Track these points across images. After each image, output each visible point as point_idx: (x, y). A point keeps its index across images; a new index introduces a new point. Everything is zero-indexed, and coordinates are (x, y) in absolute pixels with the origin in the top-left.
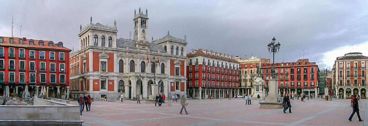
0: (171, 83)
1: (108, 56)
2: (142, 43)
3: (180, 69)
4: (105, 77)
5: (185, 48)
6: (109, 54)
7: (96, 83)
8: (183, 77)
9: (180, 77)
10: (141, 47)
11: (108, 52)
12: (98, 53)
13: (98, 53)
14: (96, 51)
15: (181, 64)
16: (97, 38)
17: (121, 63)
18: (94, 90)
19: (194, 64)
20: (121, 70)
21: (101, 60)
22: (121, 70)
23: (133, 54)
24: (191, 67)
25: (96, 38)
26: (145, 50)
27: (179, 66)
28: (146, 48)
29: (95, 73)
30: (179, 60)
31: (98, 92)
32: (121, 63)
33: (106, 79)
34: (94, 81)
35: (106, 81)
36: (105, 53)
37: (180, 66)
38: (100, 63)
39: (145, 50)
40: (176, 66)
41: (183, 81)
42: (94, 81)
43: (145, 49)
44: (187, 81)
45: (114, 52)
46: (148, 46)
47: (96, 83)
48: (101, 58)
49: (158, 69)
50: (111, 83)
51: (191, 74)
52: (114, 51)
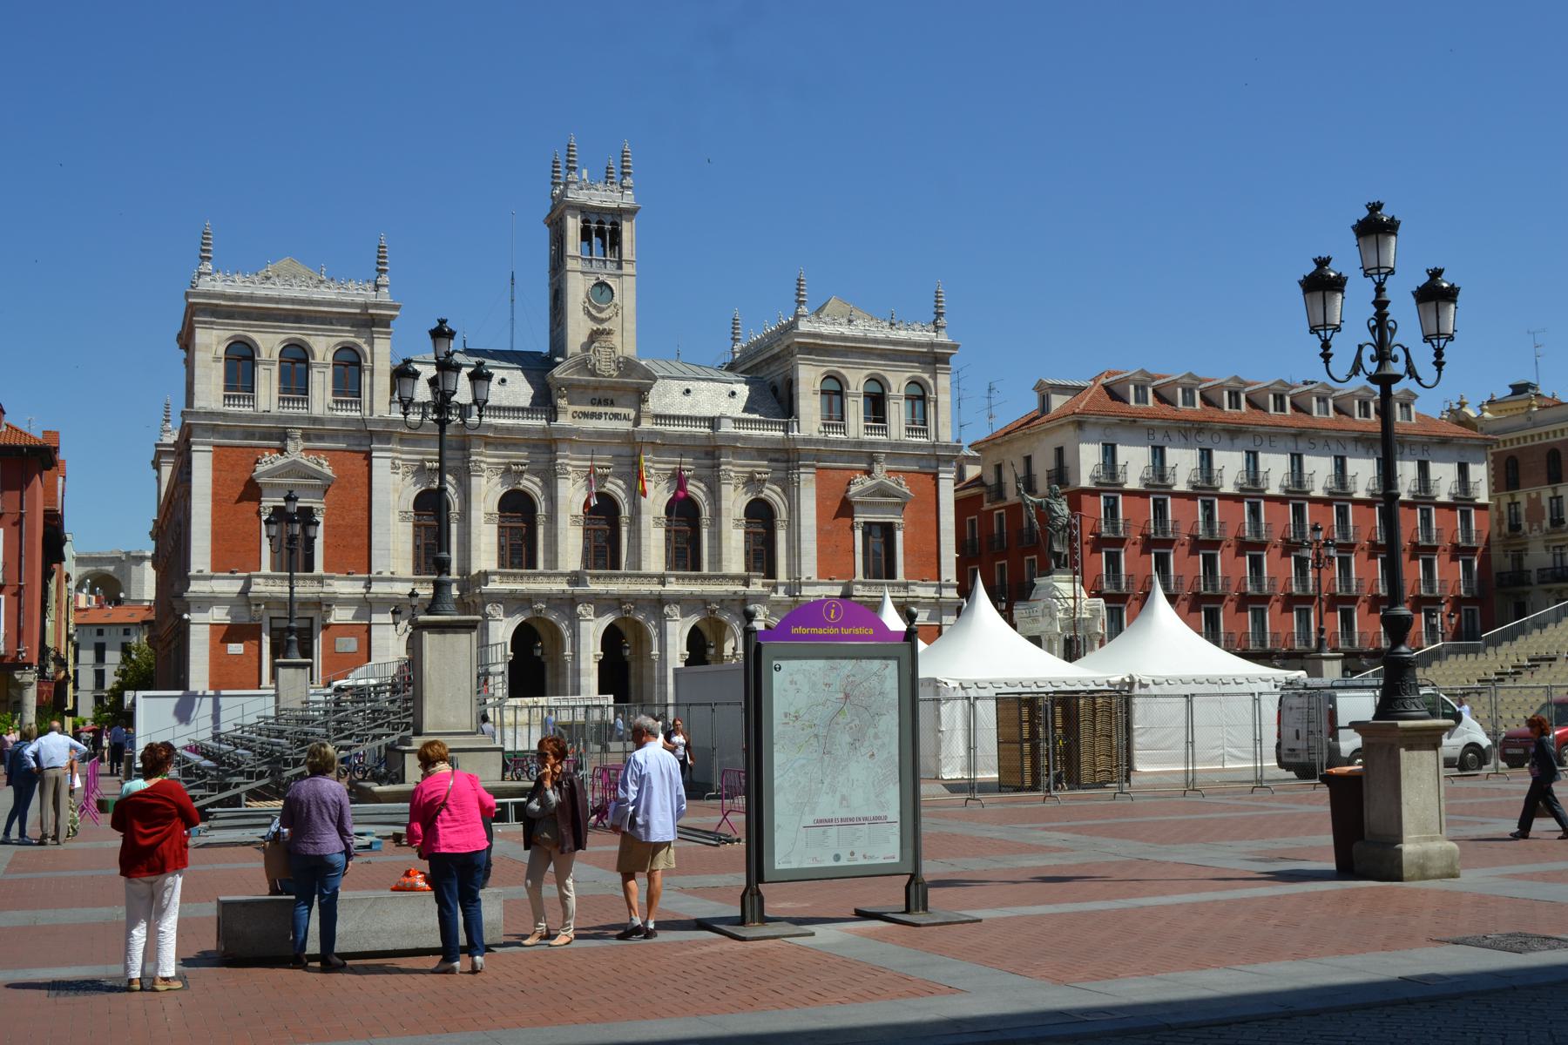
3: (899, 535)
47: (236, 648)
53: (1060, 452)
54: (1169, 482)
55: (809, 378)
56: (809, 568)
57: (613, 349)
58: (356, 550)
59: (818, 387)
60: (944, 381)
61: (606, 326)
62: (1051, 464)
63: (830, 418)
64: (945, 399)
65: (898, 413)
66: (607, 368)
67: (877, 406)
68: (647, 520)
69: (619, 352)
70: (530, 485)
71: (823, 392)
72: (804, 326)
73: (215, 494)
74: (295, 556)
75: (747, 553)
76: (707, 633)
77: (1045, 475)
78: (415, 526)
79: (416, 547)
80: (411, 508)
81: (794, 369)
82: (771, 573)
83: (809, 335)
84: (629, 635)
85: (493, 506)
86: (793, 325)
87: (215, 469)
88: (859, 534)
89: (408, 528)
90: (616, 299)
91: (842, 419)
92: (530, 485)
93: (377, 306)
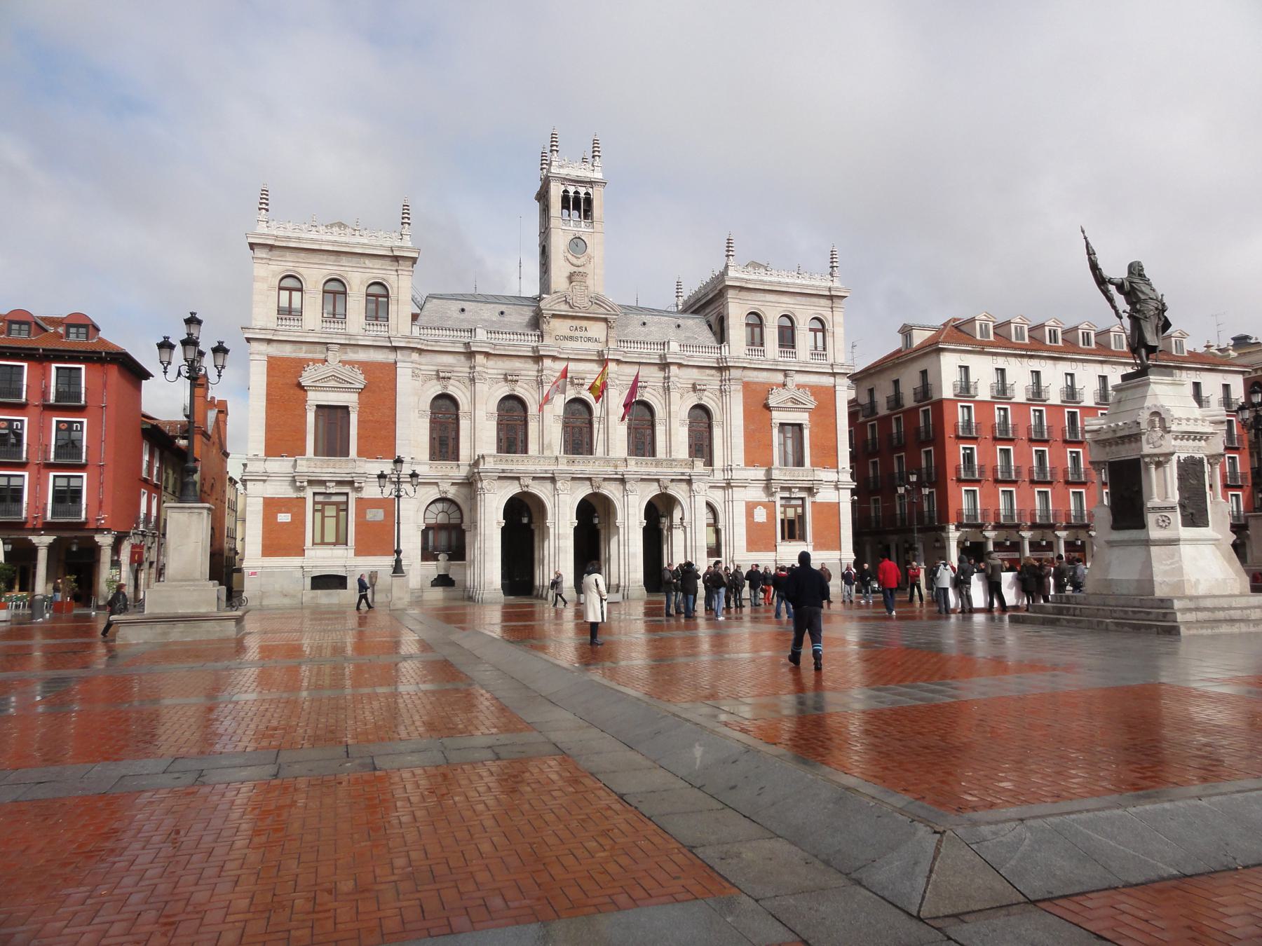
0: (750, 508)
1: (362, 377)
2: (566, 307)
3: (806, 433)
4: (339, 483)
5: (838, 321)
6: (365, 367)
7: (284, 518)
8: (828, 475)
9: (805, 474)
10: (561, 327)
11: (362, 356)
12: (300, 365)
13: (300, 365)
14: (287, 351)
15: (809, 406)
16: (301, 290)
17: (445, 413)
18: (270, 549)
19: (909, 401)
20: (444, 443)
21: (315, 398)
22: (444, 443)
23: (517, 364)
24: (898, 419)
25: (290, 290)
26: (589, 339)
27: (802, 418)
28: (597, 330)
29: (280, 465)
30: (799, 387)
31: (296, 561)
32: (445, 413)
33: (347, 494)
34: (272, 506)
35: (347, 503)
36: (344, 363)
37: (806, 415)
38: (311, 417)
39: (589, 339)
40: (778, 417)
41: (826, 495)
42: (272, 506)
43: (589, 334)
44: (854, 492)
45: (400, 355)
46: (605, 320)
47: (284, 518)
48: (316, 389)
49: (674, 436)
50: (376, 515)
51: (900, 458)
52: (395, 349)
53: (924, 373)
54: (1009, 395)
55: (737, 312)
56: (739, 456)
57: (587, 287)
58: (381, 439)
59: (744, 321)
60: (839, 317)
61: (581, 269)
62: (917, 383)
63: (753, 344)
64: (840, 331)
65: (804, 339)
66: (582, 302)
67: (787, 338)
68: (675, 424)
69: (591, 289)
70: (522, 391)
71: (747, 325)
72: (731, 273)
73: (268, 395)
74: (333, 444)
75: (690, 446)
76: (661, 509)
77: (912, 392)
78: (432, 422)
79: (432, 439)
80: (428, 408)
81: (725, 305)
82: (710, 463)
83: (737, 279)
84: (600, 509)
85: (493, 406)
86: (724, 273)
87: (268, 375)
88: (775, 431)
89: (425, 425)
90: (589, 250)
91: (762, 345)
92: (522, 391)
93: (401, 248)
